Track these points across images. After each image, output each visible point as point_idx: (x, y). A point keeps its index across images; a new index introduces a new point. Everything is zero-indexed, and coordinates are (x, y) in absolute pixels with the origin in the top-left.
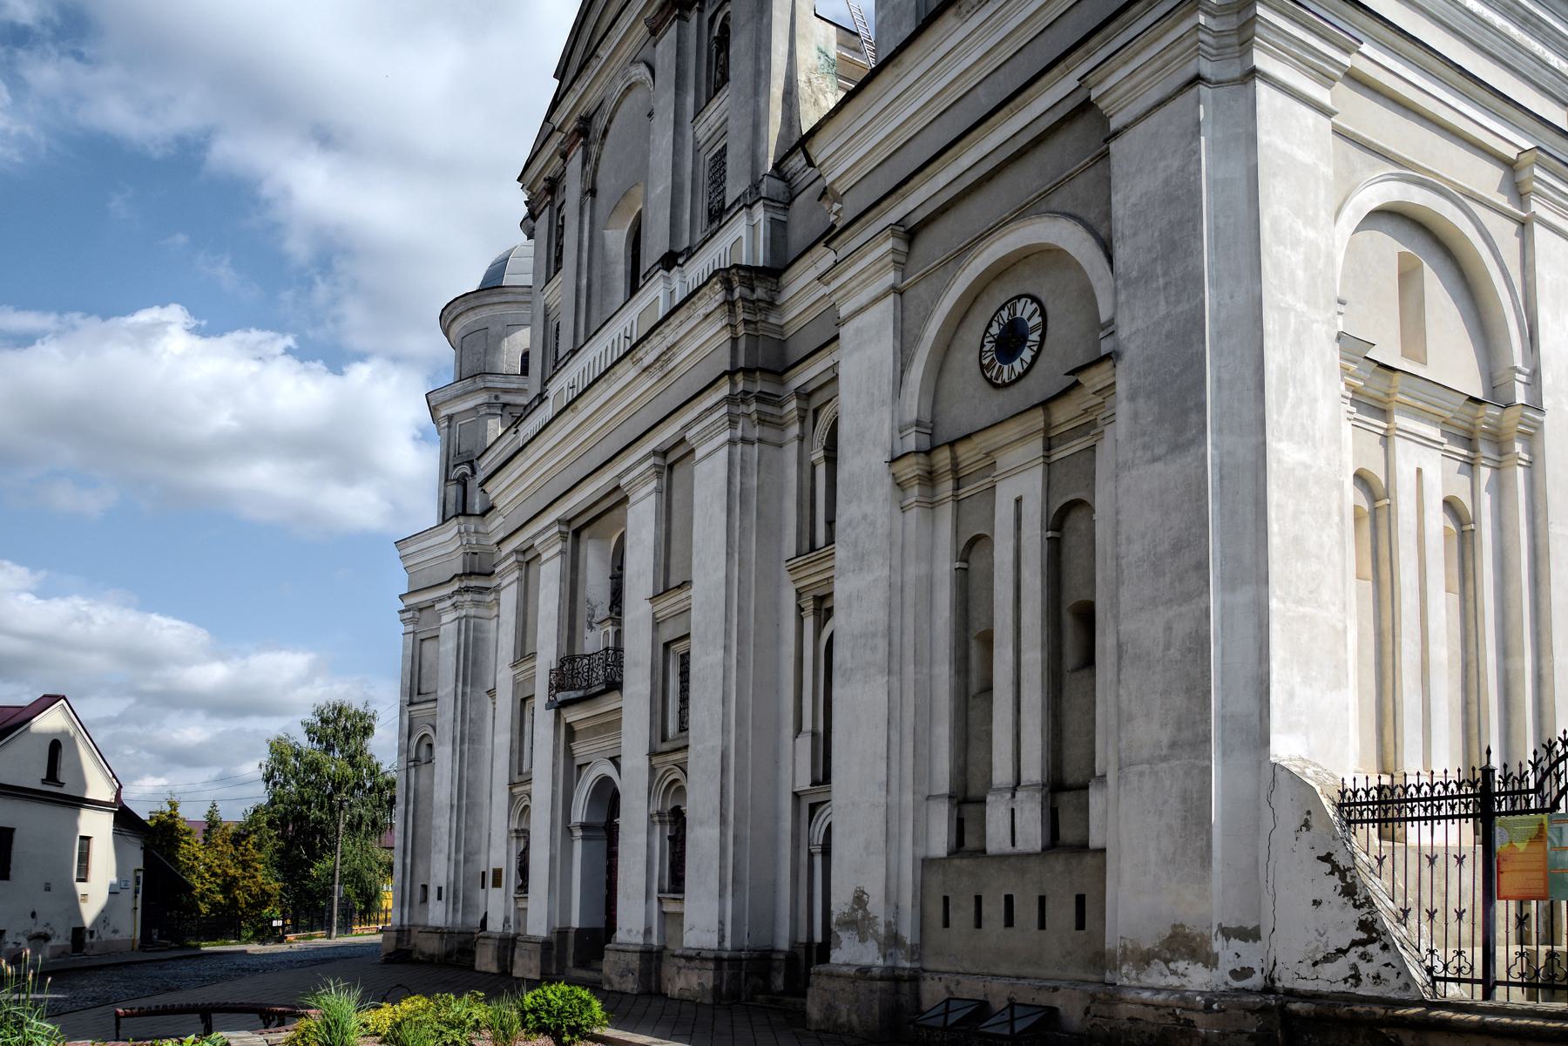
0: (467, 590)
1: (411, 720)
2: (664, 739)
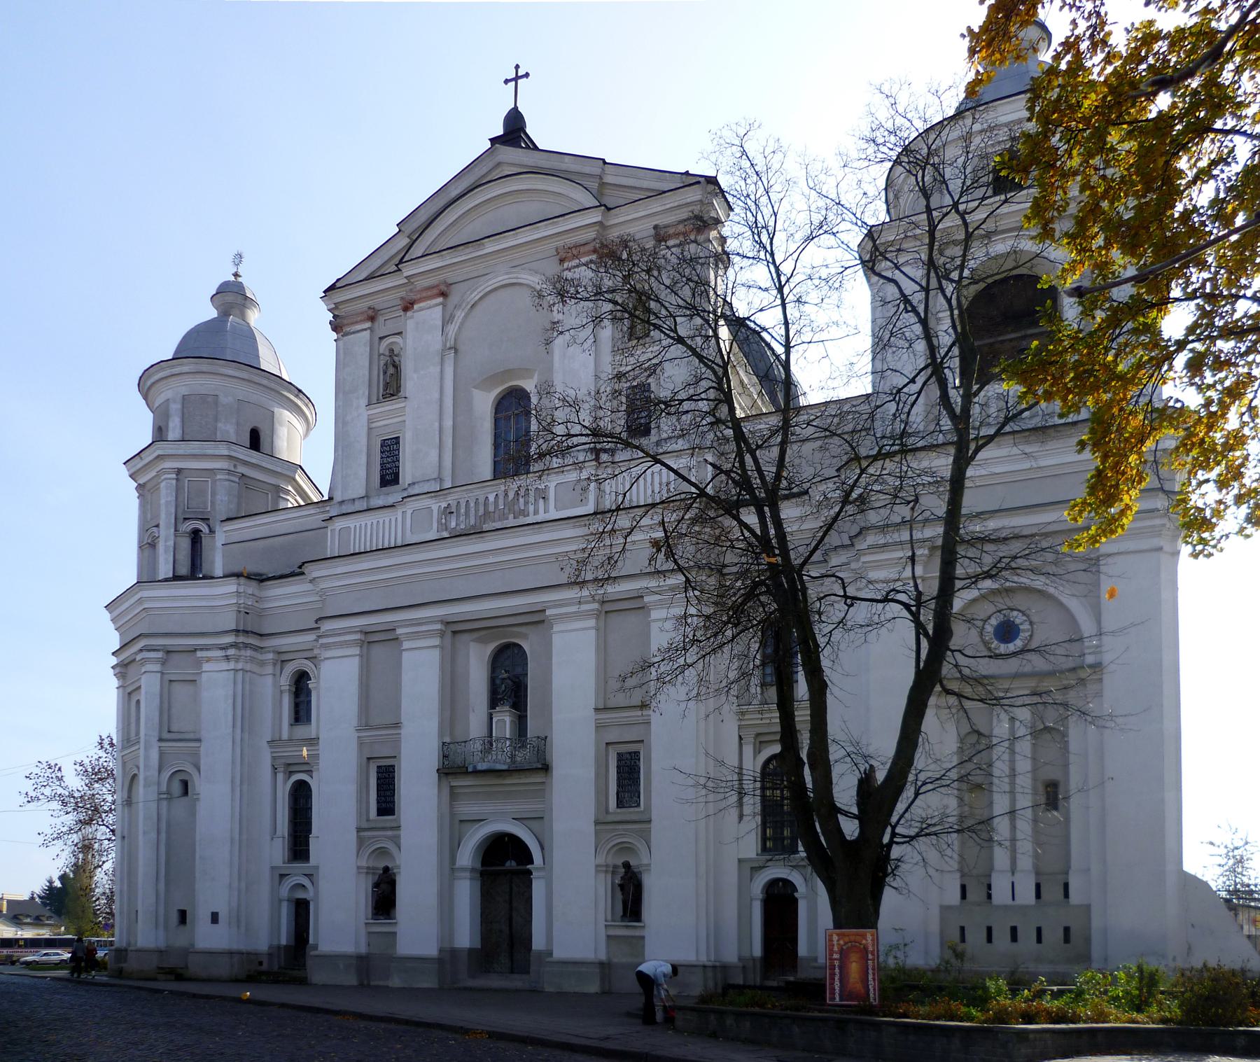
0: (246, 646)
1: (162, 754)
2: (607, 812)
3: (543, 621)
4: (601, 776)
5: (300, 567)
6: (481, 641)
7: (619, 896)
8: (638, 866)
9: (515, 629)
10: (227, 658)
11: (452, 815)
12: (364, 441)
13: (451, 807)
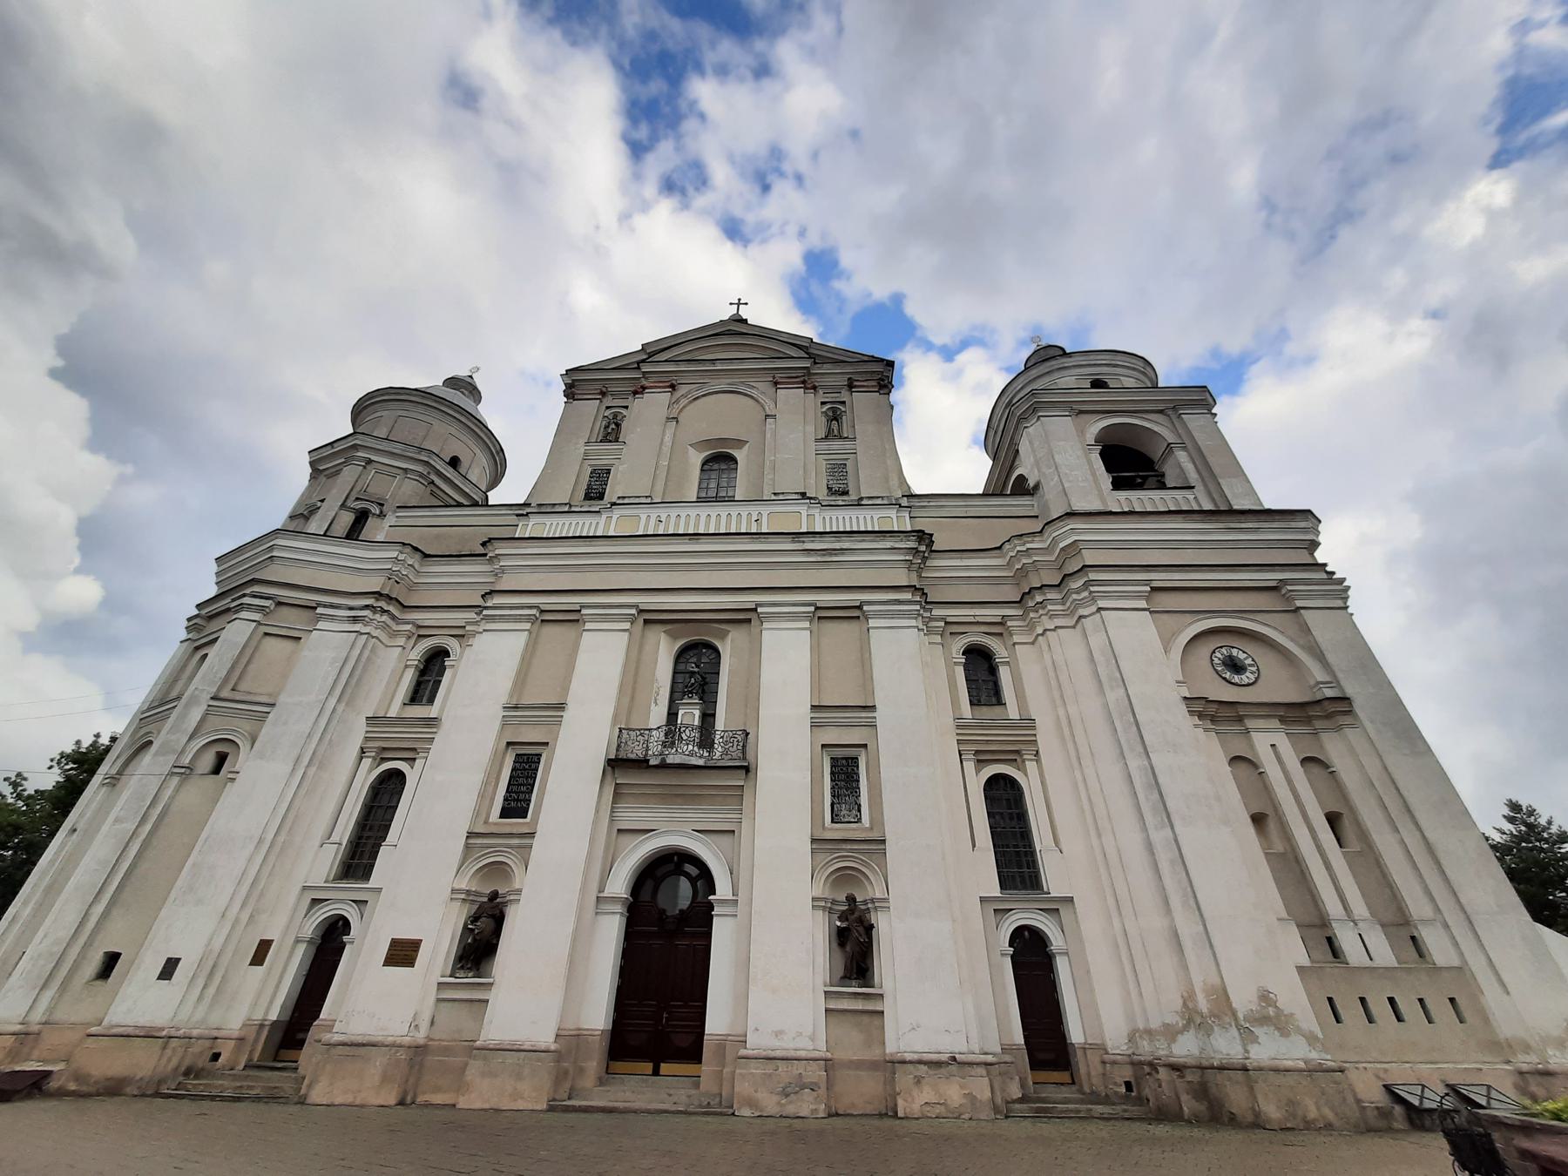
0: (384, 611)
3: (749, 621)
4: (815, 782)
5: (484, 544)
6: (673, 636)
8: (865, 902)
10: (355, 619)
11: (612, 820)
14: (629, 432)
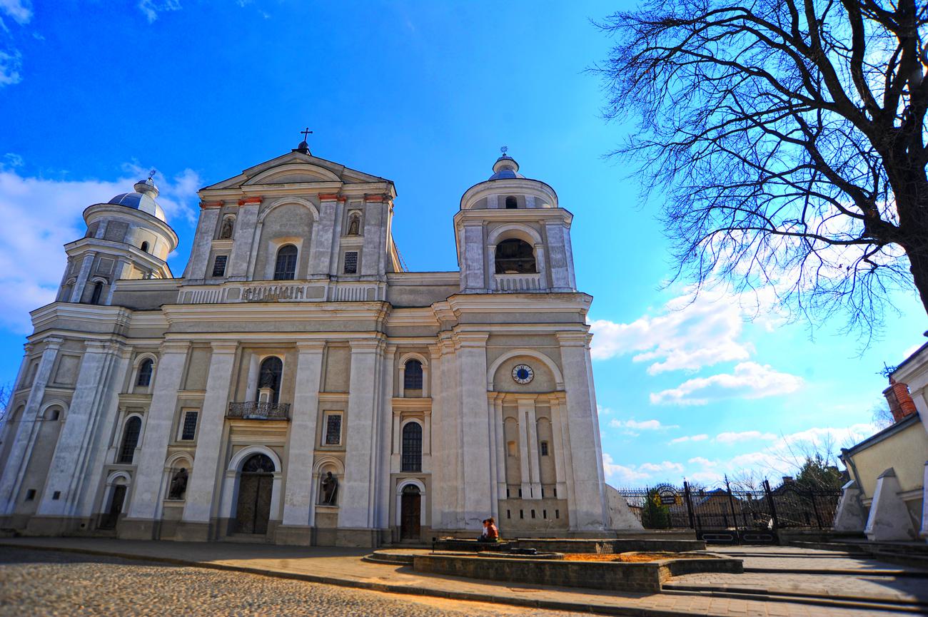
0: (117, 341)
2: (321, 445)
7: (324, 493)
8: (336, 475)
9: (278, 350)
10: (104, 347)
11: (229, 441)
12: (208, 255)
13: (229, 437)
14: (238, 232)
